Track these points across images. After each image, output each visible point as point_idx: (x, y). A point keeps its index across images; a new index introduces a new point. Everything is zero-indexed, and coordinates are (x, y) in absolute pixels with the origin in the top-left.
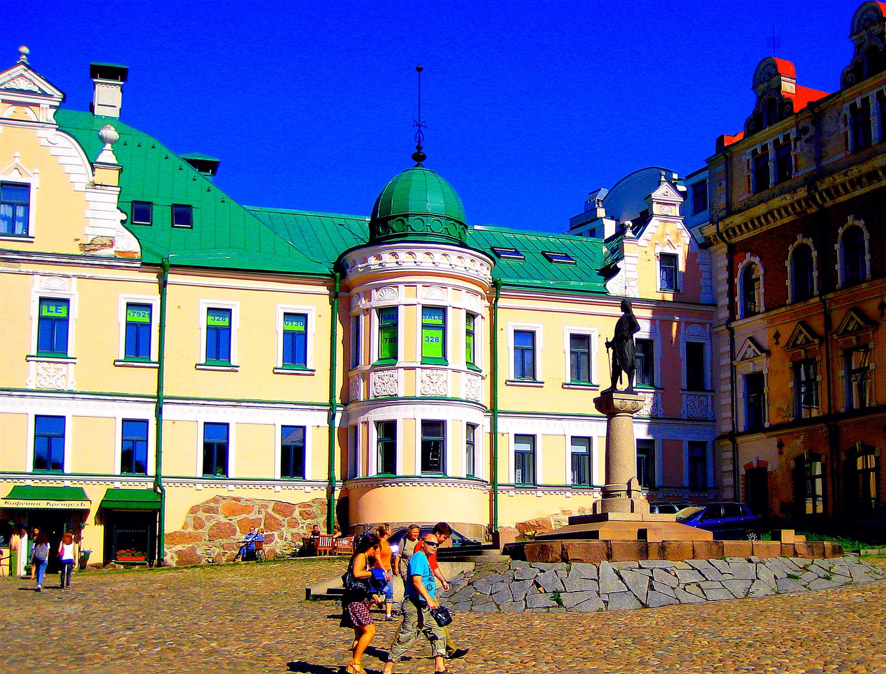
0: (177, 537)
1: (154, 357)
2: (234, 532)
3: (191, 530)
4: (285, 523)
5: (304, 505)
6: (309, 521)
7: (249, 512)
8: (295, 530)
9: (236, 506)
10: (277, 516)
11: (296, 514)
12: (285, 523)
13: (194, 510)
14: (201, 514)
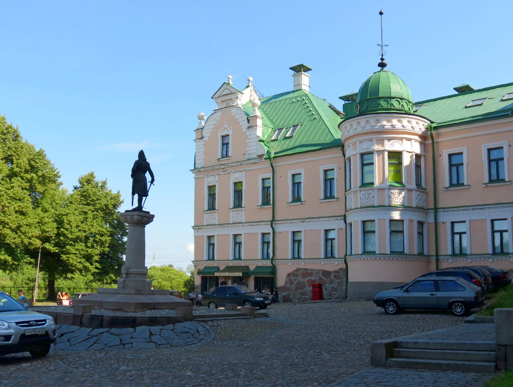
0: (284, 288)
1: (271, 203)
2: (305, 287)
3: (288, 285)
4: (328, 282)
5: (336, 272)
6: (338, 281)
7: (311, 276)
8: (332, 285)
9: (306, 273)
10: (323, 278)
11: (332, 276)
12: (328, 282)
13: (289, 275)
14: (292, 278)
